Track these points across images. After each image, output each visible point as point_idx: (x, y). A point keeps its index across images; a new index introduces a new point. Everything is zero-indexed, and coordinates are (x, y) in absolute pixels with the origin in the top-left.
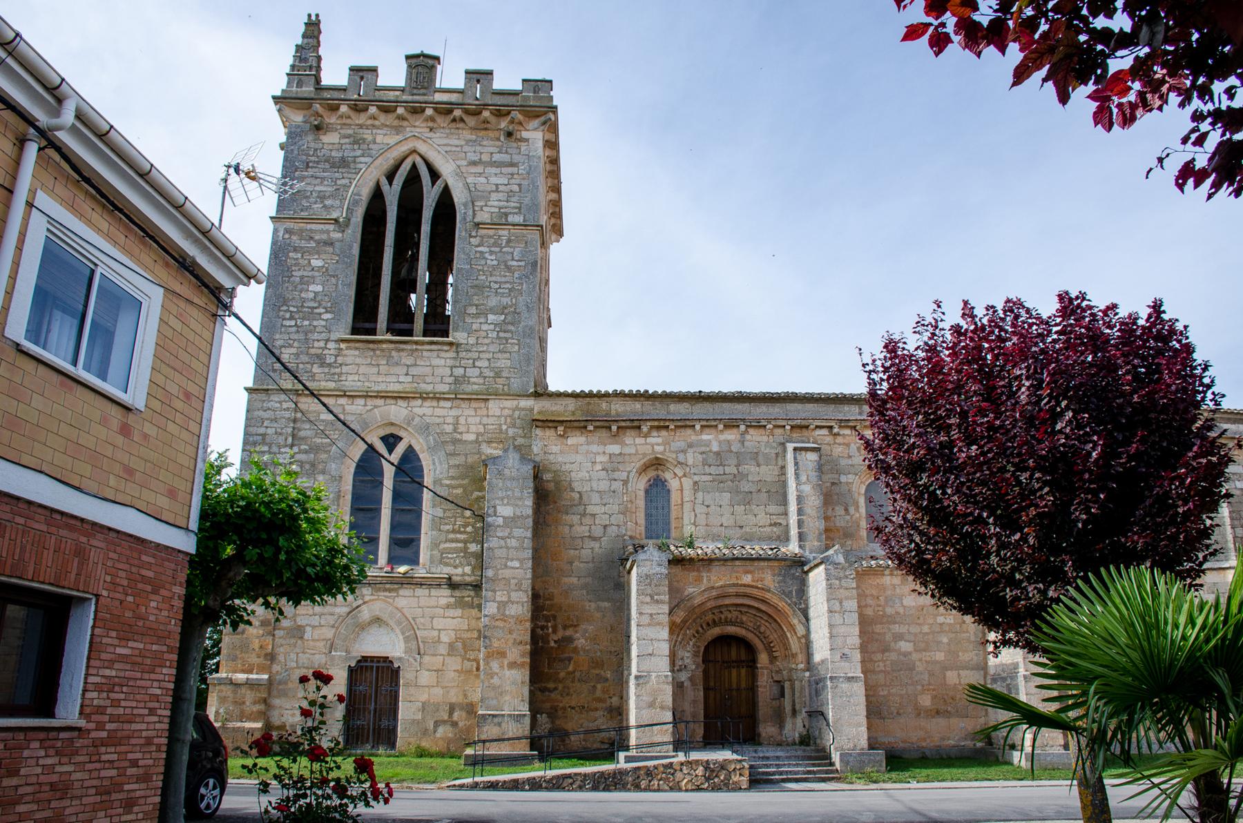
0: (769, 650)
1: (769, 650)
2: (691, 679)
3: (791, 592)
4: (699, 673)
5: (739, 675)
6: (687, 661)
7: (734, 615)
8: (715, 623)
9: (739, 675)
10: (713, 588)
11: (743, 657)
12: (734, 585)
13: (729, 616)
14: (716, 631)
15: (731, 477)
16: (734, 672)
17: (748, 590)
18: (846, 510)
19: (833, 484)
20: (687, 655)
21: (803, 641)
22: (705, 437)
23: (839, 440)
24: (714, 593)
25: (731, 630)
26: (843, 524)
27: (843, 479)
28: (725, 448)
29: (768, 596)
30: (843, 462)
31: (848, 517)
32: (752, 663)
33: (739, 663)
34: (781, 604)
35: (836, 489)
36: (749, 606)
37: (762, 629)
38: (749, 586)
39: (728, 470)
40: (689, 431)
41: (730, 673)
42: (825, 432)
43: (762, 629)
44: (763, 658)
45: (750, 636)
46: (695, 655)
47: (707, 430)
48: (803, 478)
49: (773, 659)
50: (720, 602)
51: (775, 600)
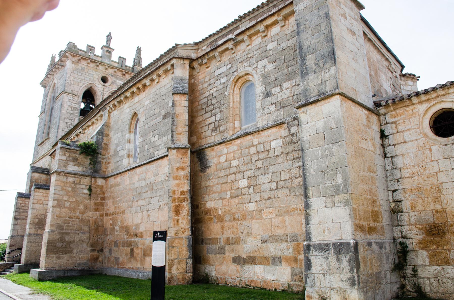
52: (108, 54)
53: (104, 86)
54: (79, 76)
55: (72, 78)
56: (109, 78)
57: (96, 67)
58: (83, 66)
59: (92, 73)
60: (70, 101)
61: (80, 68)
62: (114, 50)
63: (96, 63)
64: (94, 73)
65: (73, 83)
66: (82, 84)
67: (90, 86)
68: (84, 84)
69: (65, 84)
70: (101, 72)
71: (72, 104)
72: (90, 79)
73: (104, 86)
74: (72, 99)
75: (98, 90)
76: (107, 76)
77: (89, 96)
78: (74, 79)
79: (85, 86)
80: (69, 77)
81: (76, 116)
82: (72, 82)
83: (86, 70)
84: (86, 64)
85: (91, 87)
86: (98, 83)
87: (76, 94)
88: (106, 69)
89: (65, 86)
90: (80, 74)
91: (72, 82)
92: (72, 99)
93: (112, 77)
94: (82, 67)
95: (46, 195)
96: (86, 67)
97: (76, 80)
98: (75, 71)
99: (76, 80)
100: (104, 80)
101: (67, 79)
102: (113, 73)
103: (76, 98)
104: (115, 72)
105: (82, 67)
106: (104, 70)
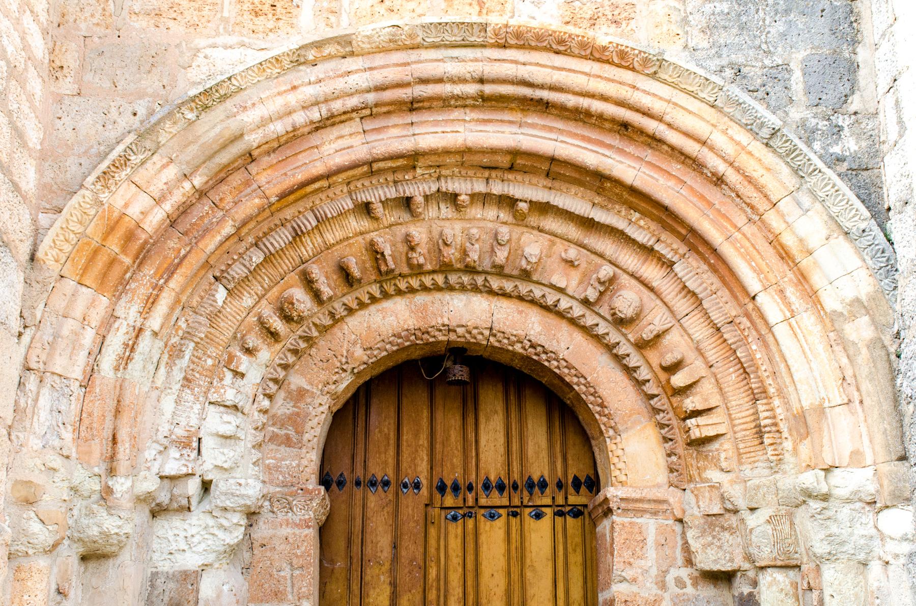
0: (670, 402)
1: (670, 402)
2: (245, 554)
3: (778, 74)
4: (294, 533)
5: (517, 555)
6: (213, 456)
7: (472, 231)
8: (385, 276)
9: (517, 555)
10: (346, 47)
11: (539, 468)
12: (469, 37)
13: (454, 230)
14: (393, 320)
16: (493, 534)
17: (541, 68)
20: (218, 422)
21: (860, 330)
24: (357, 78)
25: (467, 314)
29: (649, 93)
32: (582, 497)
33: (518, 494)
34: (728, 144)
36: (554, 169)
37: (627, 299)
38: (557, 45)
41: (472, 546)
43: (627, 299)
44: (635, 457)
45: (568, 350)
46: (279, 433)
49: (689, 448)
50: (396, 138)
51: (684, 115)
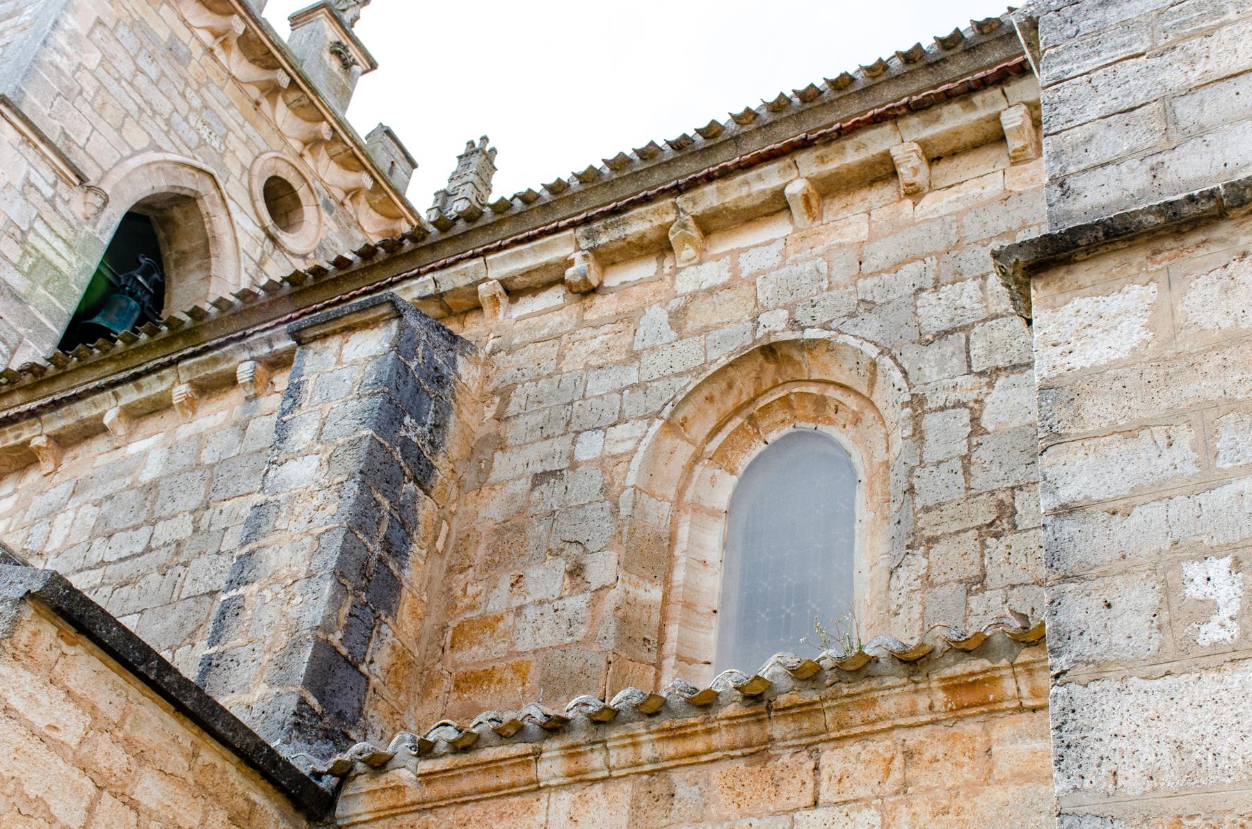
15: (163, 556)
18: (576, 571)
19: (540, 479)
22: (135, 448)
23: (602, 306)
26: (548, 636)
27: (589, 447)
28: (182, 459)
30: (599, 385)
31: (577, 602)
35: (550, 495)
39: (164, 532)
40: (99, 444)
42: (553, 297)
47: (151, 424)
48: (303, 435)
52: (335, 65)
53: (273, 239)
54: (141, 81)
55: (93, 59)
56: (309, 212)
57: (255, 93)
58: (184, 34)
59: (220, 110)
60: (34, 196)
61: (164, 35)
62: (373, 66)
63: (275, 66)
64: (232, 117)
65: (90, 91)
66: (143, 142)
67: (188, 183)
68: (159, 149)
69: (36, 61)
70: (276, 142)
71: (38, 225)
72: (202, 143)
73: (273, 239)
74: (49, 192)
75: (227, 240)
76: (302, 191)
77: (149, 241)
78: (101, 73)
79: (160, 166)
80: (74, 37)
81: (42, 330)
82: (89, 85)
83: (193, 69)
84: (207, 38)
85: (185, 201)
86: (244, 200)
87: (92, 175)
88: (314, 143)
89: (29, 74)
90: (153, 72)
91: (89, 85)
92: (49, 192)
93: (325, 215)
94: (173, 37)
95: (119, 759)
96: (198, 52)
97: (114, 88)
98: (122, 31)
99: (114, 88)
100: (280, 200)
101: (61, 40)
102: (340, 195)
103: (78, 204)
104: (353, 193)
105: (173, 37)
106: (297, 146)
